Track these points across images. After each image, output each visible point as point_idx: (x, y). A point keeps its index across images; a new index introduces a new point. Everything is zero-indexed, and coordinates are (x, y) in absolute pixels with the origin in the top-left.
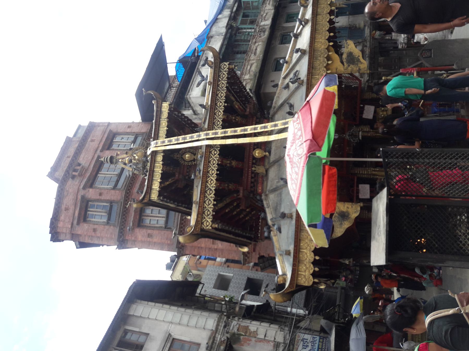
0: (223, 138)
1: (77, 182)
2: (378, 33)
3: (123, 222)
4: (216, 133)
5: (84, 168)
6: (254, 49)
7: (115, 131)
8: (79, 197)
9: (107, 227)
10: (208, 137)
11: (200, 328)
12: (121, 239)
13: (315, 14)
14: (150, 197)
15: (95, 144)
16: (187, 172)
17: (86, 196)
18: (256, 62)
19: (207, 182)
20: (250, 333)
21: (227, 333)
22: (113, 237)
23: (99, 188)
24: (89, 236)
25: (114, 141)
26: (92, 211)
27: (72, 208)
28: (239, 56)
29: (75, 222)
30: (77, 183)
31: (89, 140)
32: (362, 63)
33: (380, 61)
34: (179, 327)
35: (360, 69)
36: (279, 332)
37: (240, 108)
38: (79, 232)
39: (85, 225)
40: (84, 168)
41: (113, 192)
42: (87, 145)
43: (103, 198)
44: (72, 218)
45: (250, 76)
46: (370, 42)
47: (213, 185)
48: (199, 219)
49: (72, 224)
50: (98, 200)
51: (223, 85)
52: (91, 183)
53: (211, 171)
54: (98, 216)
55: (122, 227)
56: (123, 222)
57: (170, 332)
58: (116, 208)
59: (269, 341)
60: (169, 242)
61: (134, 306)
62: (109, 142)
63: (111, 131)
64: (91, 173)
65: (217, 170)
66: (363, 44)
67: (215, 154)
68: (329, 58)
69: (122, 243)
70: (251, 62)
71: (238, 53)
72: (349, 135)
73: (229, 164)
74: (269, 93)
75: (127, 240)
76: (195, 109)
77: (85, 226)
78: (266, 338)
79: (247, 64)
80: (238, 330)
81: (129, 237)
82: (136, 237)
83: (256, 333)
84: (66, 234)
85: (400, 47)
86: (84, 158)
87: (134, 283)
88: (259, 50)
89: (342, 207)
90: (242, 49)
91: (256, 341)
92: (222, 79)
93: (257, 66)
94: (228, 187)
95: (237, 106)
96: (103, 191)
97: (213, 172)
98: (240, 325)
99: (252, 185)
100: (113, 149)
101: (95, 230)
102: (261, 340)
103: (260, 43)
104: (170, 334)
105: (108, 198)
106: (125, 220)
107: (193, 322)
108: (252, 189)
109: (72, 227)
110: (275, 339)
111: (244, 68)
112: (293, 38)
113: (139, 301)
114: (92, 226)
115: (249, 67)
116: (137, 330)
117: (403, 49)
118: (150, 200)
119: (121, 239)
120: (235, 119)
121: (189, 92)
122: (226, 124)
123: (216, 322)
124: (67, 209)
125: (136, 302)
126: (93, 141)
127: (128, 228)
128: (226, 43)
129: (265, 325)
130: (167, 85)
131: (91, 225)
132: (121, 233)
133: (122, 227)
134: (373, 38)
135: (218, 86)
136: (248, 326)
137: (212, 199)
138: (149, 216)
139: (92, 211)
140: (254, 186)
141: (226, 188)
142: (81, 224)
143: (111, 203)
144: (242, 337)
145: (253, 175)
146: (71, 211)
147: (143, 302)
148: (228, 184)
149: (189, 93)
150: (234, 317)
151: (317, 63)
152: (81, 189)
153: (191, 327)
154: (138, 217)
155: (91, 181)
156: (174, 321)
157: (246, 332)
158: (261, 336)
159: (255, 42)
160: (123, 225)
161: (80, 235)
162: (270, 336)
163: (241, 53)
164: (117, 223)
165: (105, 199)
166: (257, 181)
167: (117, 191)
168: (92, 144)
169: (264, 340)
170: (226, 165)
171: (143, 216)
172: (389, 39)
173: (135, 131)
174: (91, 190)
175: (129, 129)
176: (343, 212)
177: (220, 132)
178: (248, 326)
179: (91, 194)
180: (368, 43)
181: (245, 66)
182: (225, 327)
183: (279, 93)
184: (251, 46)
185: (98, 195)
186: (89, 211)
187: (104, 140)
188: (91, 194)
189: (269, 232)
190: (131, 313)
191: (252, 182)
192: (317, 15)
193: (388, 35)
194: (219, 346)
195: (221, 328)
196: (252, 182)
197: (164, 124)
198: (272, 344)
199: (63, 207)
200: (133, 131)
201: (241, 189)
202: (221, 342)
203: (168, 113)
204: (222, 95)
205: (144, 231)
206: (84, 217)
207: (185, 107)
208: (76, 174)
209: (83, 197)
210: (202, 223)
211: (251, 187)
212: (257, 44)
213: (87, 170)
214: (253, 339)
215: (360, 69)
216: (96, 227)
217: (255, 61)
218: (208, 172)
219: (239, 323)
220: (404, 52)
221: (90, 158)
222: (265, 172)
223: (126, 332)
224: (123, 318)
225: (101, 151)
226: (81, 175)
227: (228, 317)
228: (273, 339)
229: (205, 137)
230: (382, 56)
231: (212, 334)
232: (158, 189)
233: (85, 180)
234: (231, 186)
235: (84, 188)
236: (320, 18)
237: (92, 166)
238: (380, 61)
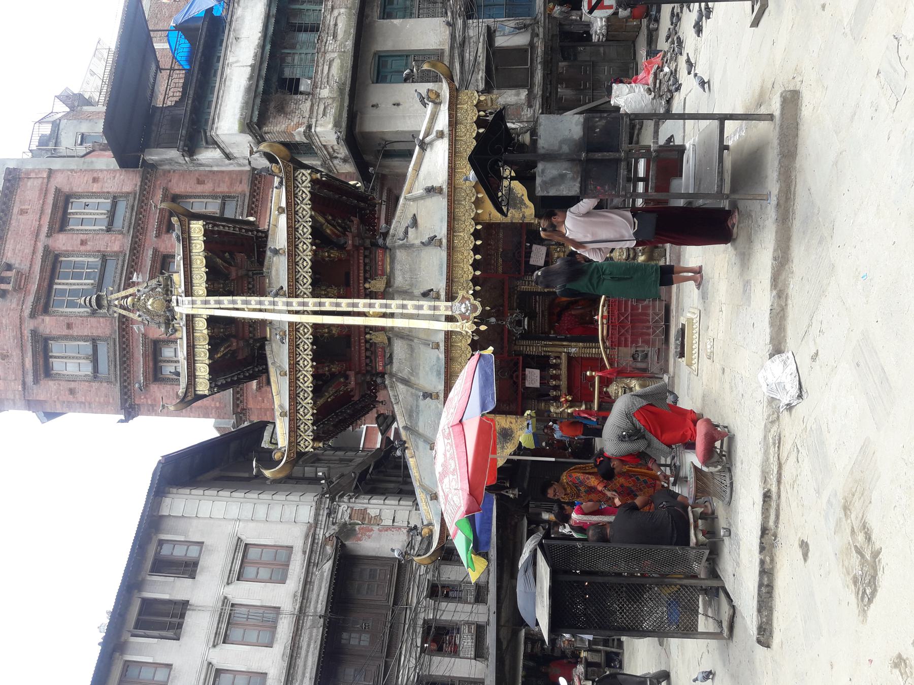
0: (315, 313)
1: (12, 302)
2: (557, 9)
3: (125, 375)
4: (304, 304)
5: (22, 274)
6: (332, 23)
7: (66, 189)
8: (27, 333)
9: (95, 385)
10: (290, 308)
11: (287, 522)
12: (127, 405)
13: (453, 122)
14: (195, 390)
16: (250, 332)
17: (41, 329)
18: (340, 56)
19: (297, 379)
20: (370, 519)
21: (333, 524)
22: (111, 401)
23: (62, 315)
24: (64, 402)
25: (69, 211)
26: (58, 357)
27: (16, 354)
28: (303, 36)
29: (30, 379)
30: (14, 305)
31: (16, 210)
32: (527, 207)
33: (560, 70)
34: (252, 525)
35: (524, 217)
36: (414, 512)
37: (334, 233)
38: (42, 398)
39: (51, 383)
40: (22, 274)
41: (93, 320)
42: (14, 223)
43: (75, 332)
44: (20, 372)
45: (330, 92)
46: (544, 28)
47: (309, 384)
48: (292, 439)
49: (24, 384)
50: (66, 338)
51: (304, 213)
52: (44, 304)
53: (301, 362)
54: (71, 364)
55: (125, 384)
56: (125, 375)
57: (239, 535)
58: (103, 349)
59: (400, 528)
60: (218, 405)
61: (167, 501)
62: (59, 214)
63: (58, 191)
64: (39, 285)
65: (312, 360)
66: (533, 30)
67: (305, 334)
68: (478, 203)
69: (130, 410)
70: (329, 56)
71: (300, 30)
72: (511, 323)
73: (328, 333)
74: (372, 133)
75: (138, 405)
76: (227, 151)
77: (52, 385)
78: (395, 524)
79: (321, 61)
80: (350, 518)
81: (140, 400)
82: (155, 400)
83: (378, 519)
84: (13, 400)
85: (595, 38)
86: (14, 250)
87: (160, 462)
88: (341, 26)
89: (503, 422)
90: (309, 19)
91: (380, 531)
92: (302, 202)
93: (342, 67)
94: (330, 370)
95: (328, 231)
96: (72, 320)
97: (306, 363)
98: (352, 509)
99: (368, 361)
100: (73, 230)
101: (72, 391)
102: (387, 528)
103: (342, 10)
104: (239, 538)
105: (86, 332)
106: (129, 372)
107: (276, 513)
108: (369, 368)
109: (24, 387)
110: (409, 523)
111: (316, 72)
112: (417, 148)
113: (175, 490)
115: (326, 68)
116: (182, 538)
117: (599, 44)
118: (195, 394)
119: (127, 405)
120: (329, 256)
121: (213, 123)
122: (320, 287)
125: (169, 493)
126: (23, 212)
127: (137, 385)
128: (274, 11)
129: (392, 502)
130: (154, 67)
131: (63, 383)
132: (126, 394)
133: (125, 384)
134: (549, 16)
135: (296, 213)
136: (366, 509)
137: (309, 407)
138: (172, 362)
139: (58, 357)
140: (371, 361)
141: (327, 373)
142: (42, 382)
143: (94, 341)
144: (357, 527)
147: (182, 491)
148: (328, 366)
149: (215, 126)
150: (341, 496)
151: (460, 211)
152: (27, 319)
153: (271, 522)
154: (151, 364)
155: (42, 301)
156: (243, 517)
157: (364, 519)
158: (390, 523)
159: (333, 8)
160: (125, 381)
161: (45, 401)
162: (401, 521)
163: (306, 31)
164: (113, 377)
165: (80, 334)
166: (374, 353)
167: (101, 319)
168: (23, 218)
169: (393, 527)
170: (322, 336)
171: (161, 361)
172: (576, 20)
173: (110, 190)
174: (47, 319)
175: (95, 185)
176: (505, 429)
177: (312, 303)
178: (366, 509)
179: (49, 325)
180: (541, 30)
181: (318, 66)
182: (329, 515)
183: (400, 217)
184: (325, 17)
185: (65, 327)
186: (51, 357)
187: (48, 210)
189: (404, 451)
190: (165, 511)
191: (367, 357)
192: (456, 124)
193: (574, 12)
194: (323, 546)
195: (323, 518)
196: (367, 357)
197: (199, 262)
198: (405, 531)
200: (105, 190)
201: (352, 374)
202: (326, 540)
203: (204, 241)
204: (305, 230)
206: (44, 368)
207: (207, 143)
208: (9, 287)
209: (34, 333)
210: (298, 444)
211: (367, 365)
212: (336, 13)
213: (28, 278)
214: (376, 528)
215: (524, 217)
216: (72, 385)
217: (336, 54)
218: (297, 363)
219: (351, 505)
220: (602, 49)
221: (28, 251)
222: (387, 342)
223: (161, 543)
224: (151, 523)
225: (49, 235)
226: (18, 289)
227: (332, 500)
228: (405, 524)
229: (285, 308)
230: (565, 59)
231: (309, 529)
232: (207, 377)
233: (31, 299)
234: (335, 369)
235: (33, 315)
236: (461, 129)
238: (560, 70)
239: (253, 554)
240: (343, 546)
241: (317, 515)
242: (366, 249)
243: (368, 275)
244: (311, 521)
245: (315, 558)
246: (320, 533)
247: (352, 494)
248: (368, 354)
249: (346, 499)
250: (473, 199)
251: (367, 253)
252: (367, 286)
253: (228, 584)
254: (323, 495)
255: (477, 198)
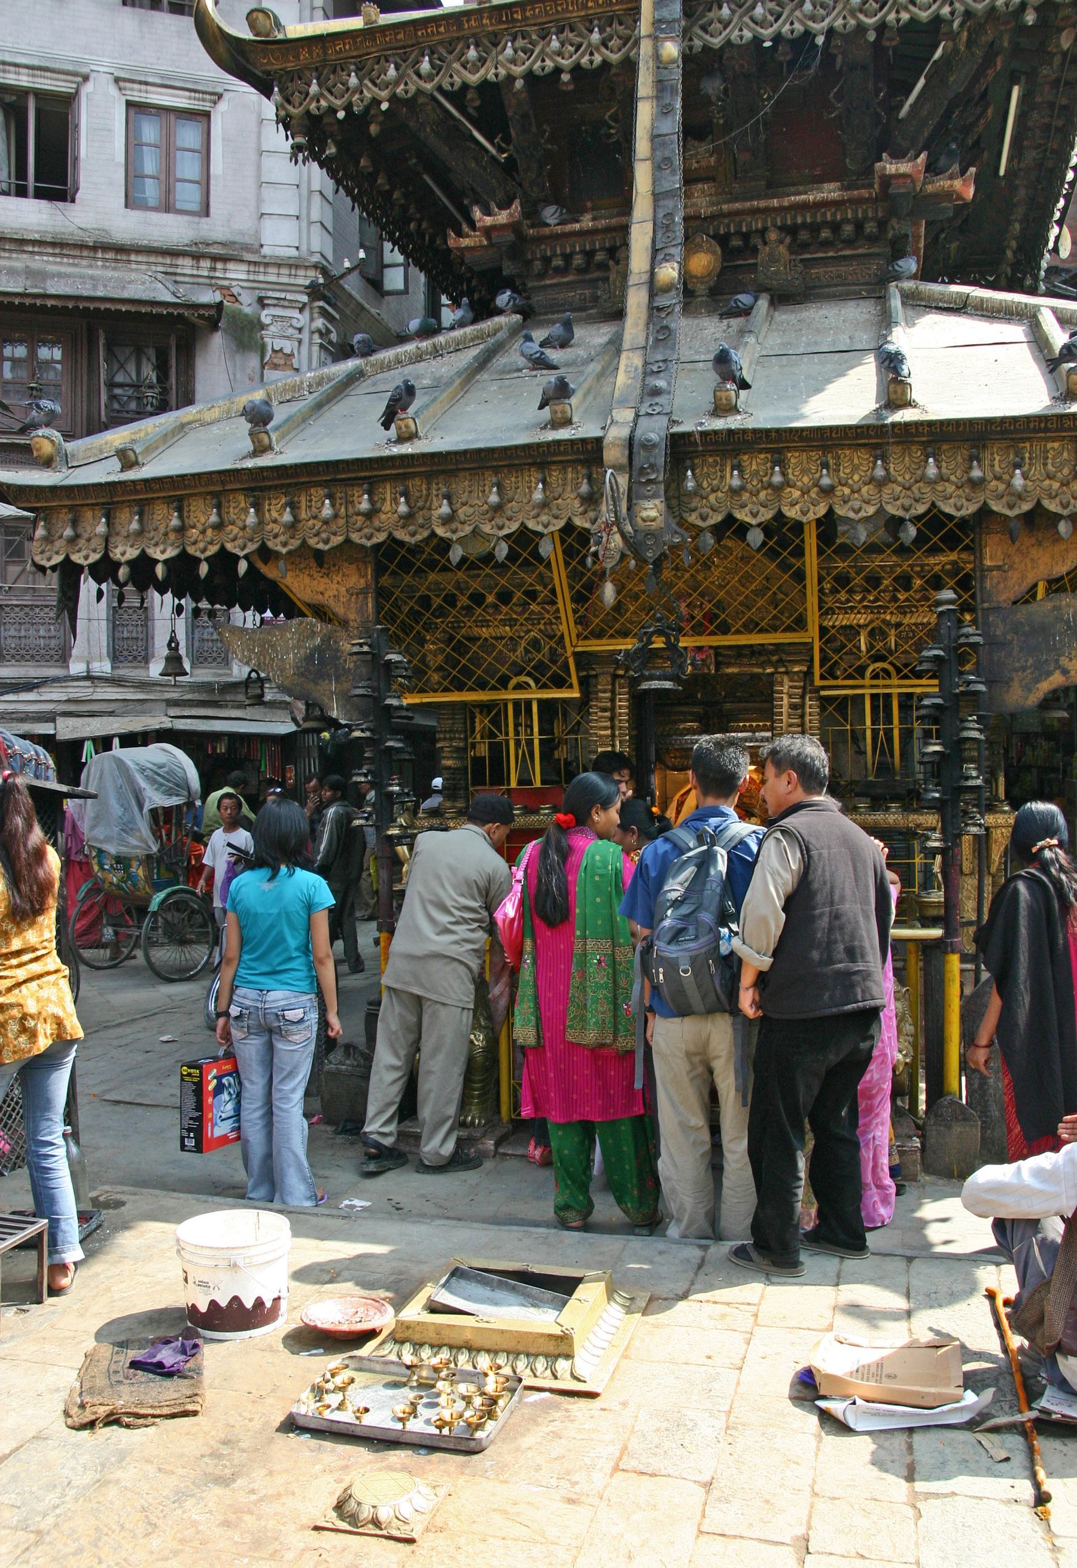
21: (261, 302)
99: (558, 262)
123: (293, 253)
145: (600, 257)
196: (568, 258)
211: (547, 260)
231: (246, 248)
239: (188, 135)
240: (213, 325)
241: (279, 264)
242: (882, 225)
243: (804, 236)
244: (265, 251)
245: (186, 265)
246: (237, 273)
247: (334, 337)
248: (578, 260)
249: (320, 323)
250: (1052, 506)
251: (870, 228)
252: (773, 236)
253: (117, 80)
254: (324, 271)
255: (1058, 517)
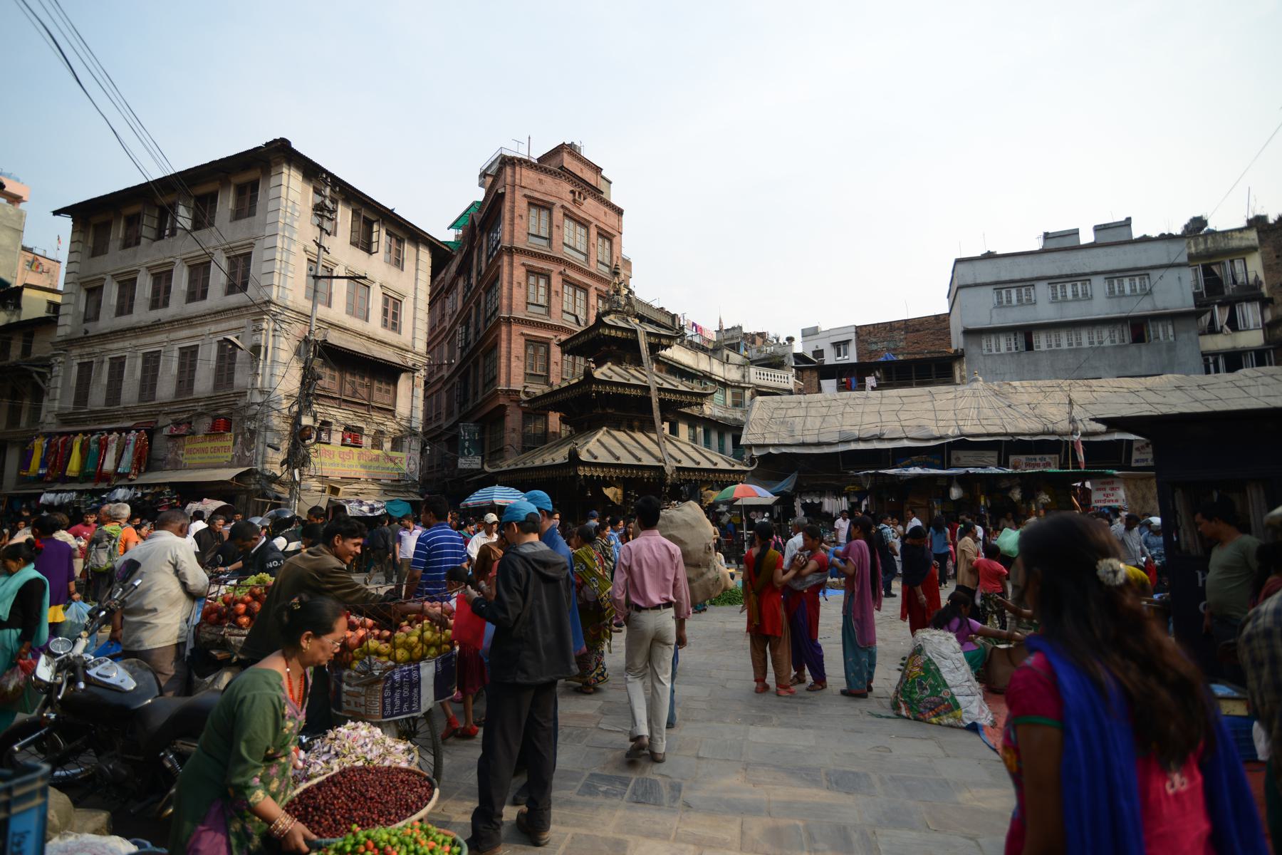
7: (615, 240)
8: (552, 200)
15: (602, 218)
43: (555, 229)
114: (525, 213)
124: (540, 181)
146: (538, 187)
188: (558, 214)
199: (542, 177)
205: (524, 278)
235: (563, 207)
237: (582, 215)
246: (410, 355)
